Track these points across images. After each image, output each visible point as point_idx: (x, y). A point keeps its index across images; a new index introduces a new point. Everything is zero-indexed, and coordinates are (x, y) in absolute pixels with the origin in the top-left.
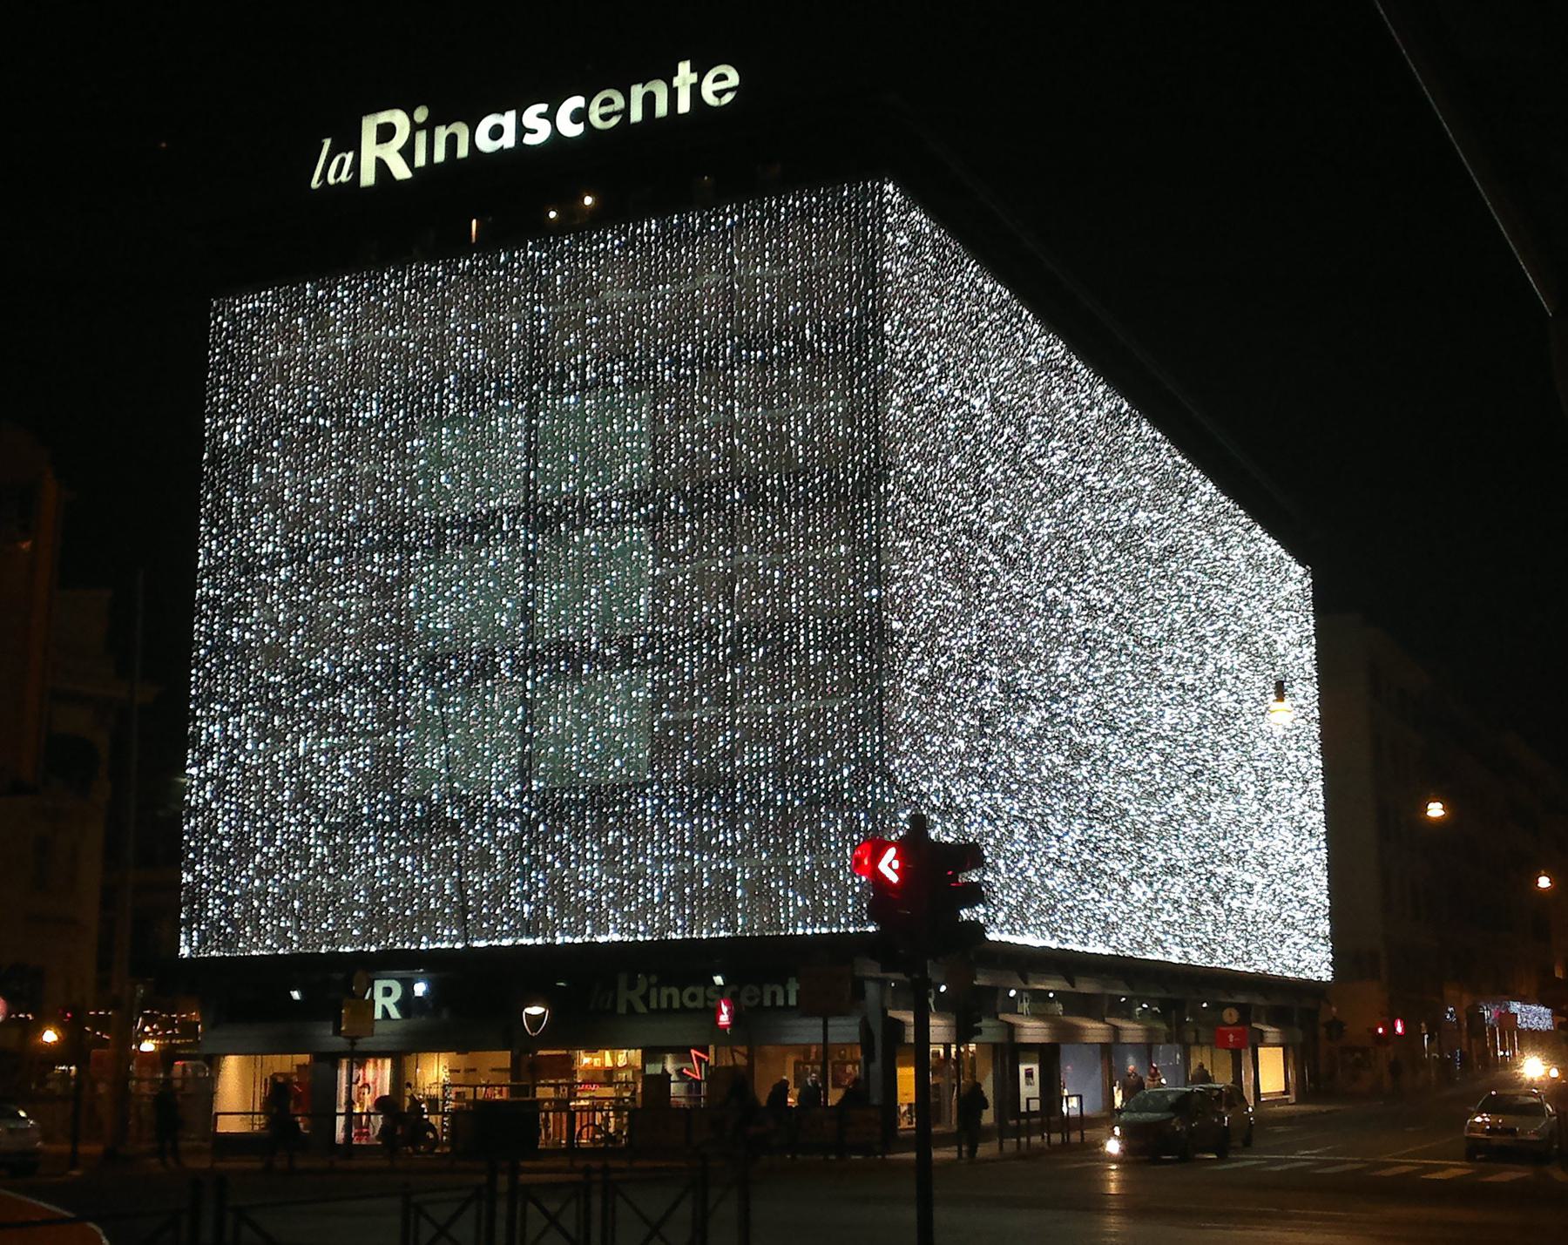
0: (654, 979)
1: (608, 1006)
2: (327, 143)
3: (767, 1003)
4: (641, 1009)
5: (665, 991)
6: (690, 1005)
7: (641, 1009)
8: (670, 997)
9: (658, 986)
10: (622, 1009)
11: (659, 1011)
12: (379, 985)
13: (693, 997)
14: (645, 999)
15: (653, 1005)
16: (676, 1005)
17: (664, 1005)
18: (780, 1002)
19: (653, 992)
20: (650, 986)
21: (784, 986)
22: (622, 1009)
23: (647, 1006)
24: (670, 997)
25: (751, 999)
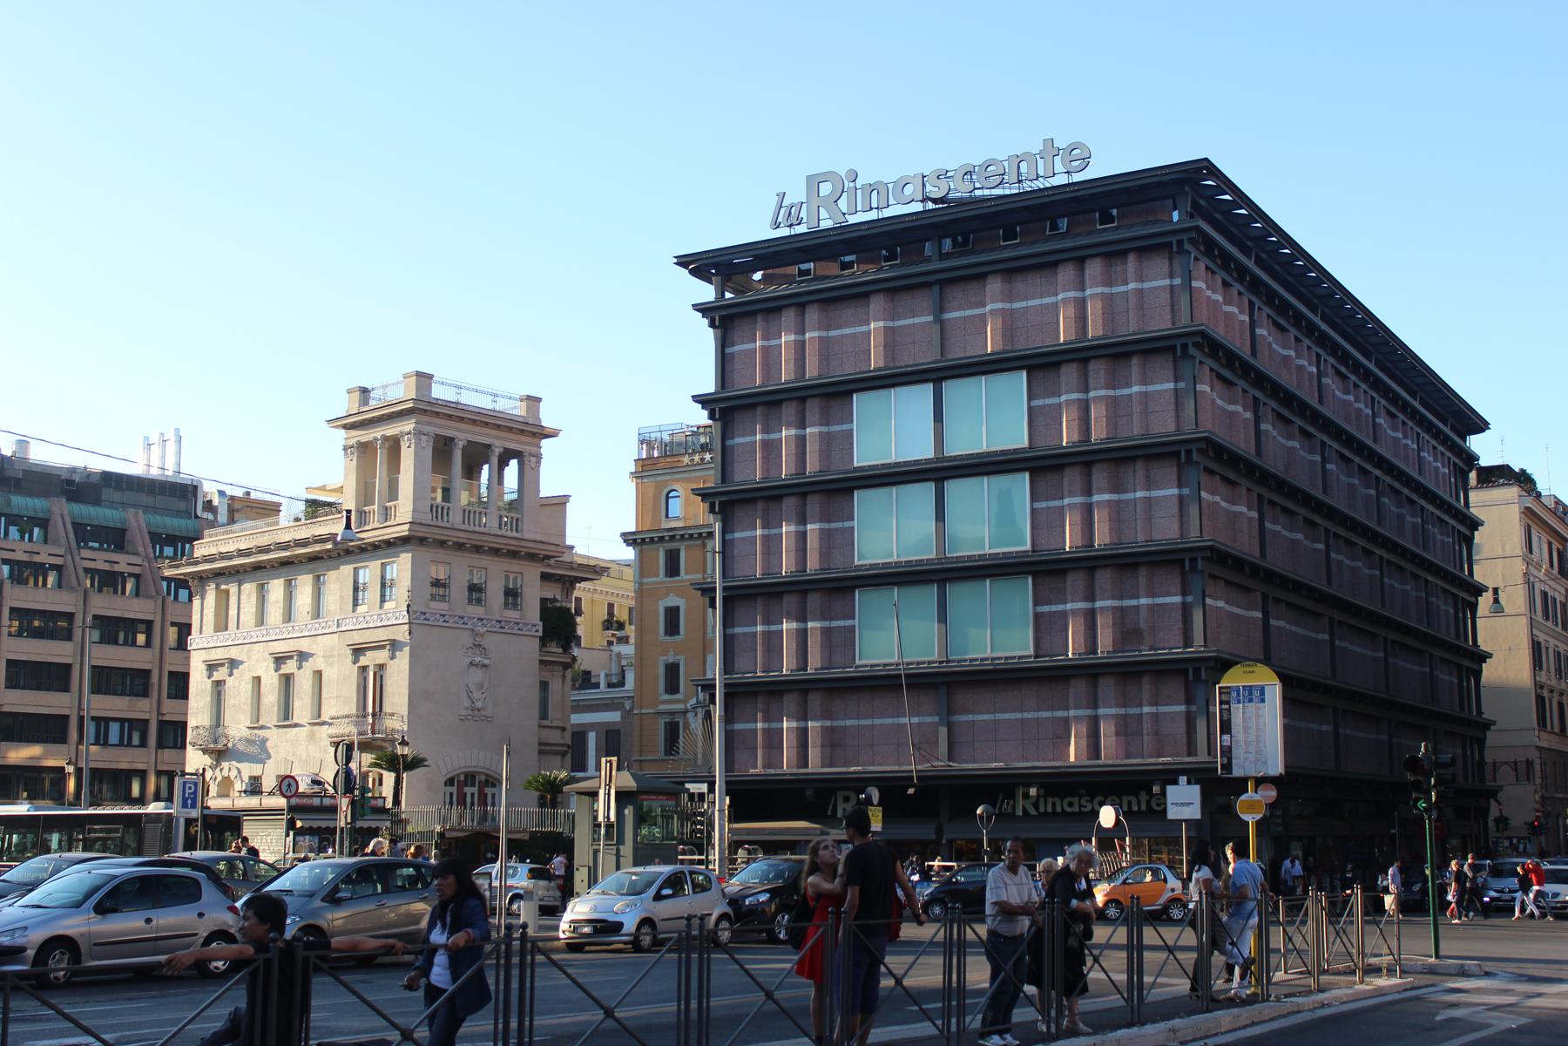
4: (1033, 812)
5: (1050, 800)
6: (1068, 809)
7: (1033, 812)
8: (1054, 805)
9: (1045, 796)
10: (1020, 813)
11: (1046, 813)
12: (840, 795)
13: (1071, 804)
14: (1036, 805)
15: (1042, 809)
16: (1059, 809)
17: (1050, 809)
19: (1042, 800)
21: (1137, 796)
24: (1054, 805)
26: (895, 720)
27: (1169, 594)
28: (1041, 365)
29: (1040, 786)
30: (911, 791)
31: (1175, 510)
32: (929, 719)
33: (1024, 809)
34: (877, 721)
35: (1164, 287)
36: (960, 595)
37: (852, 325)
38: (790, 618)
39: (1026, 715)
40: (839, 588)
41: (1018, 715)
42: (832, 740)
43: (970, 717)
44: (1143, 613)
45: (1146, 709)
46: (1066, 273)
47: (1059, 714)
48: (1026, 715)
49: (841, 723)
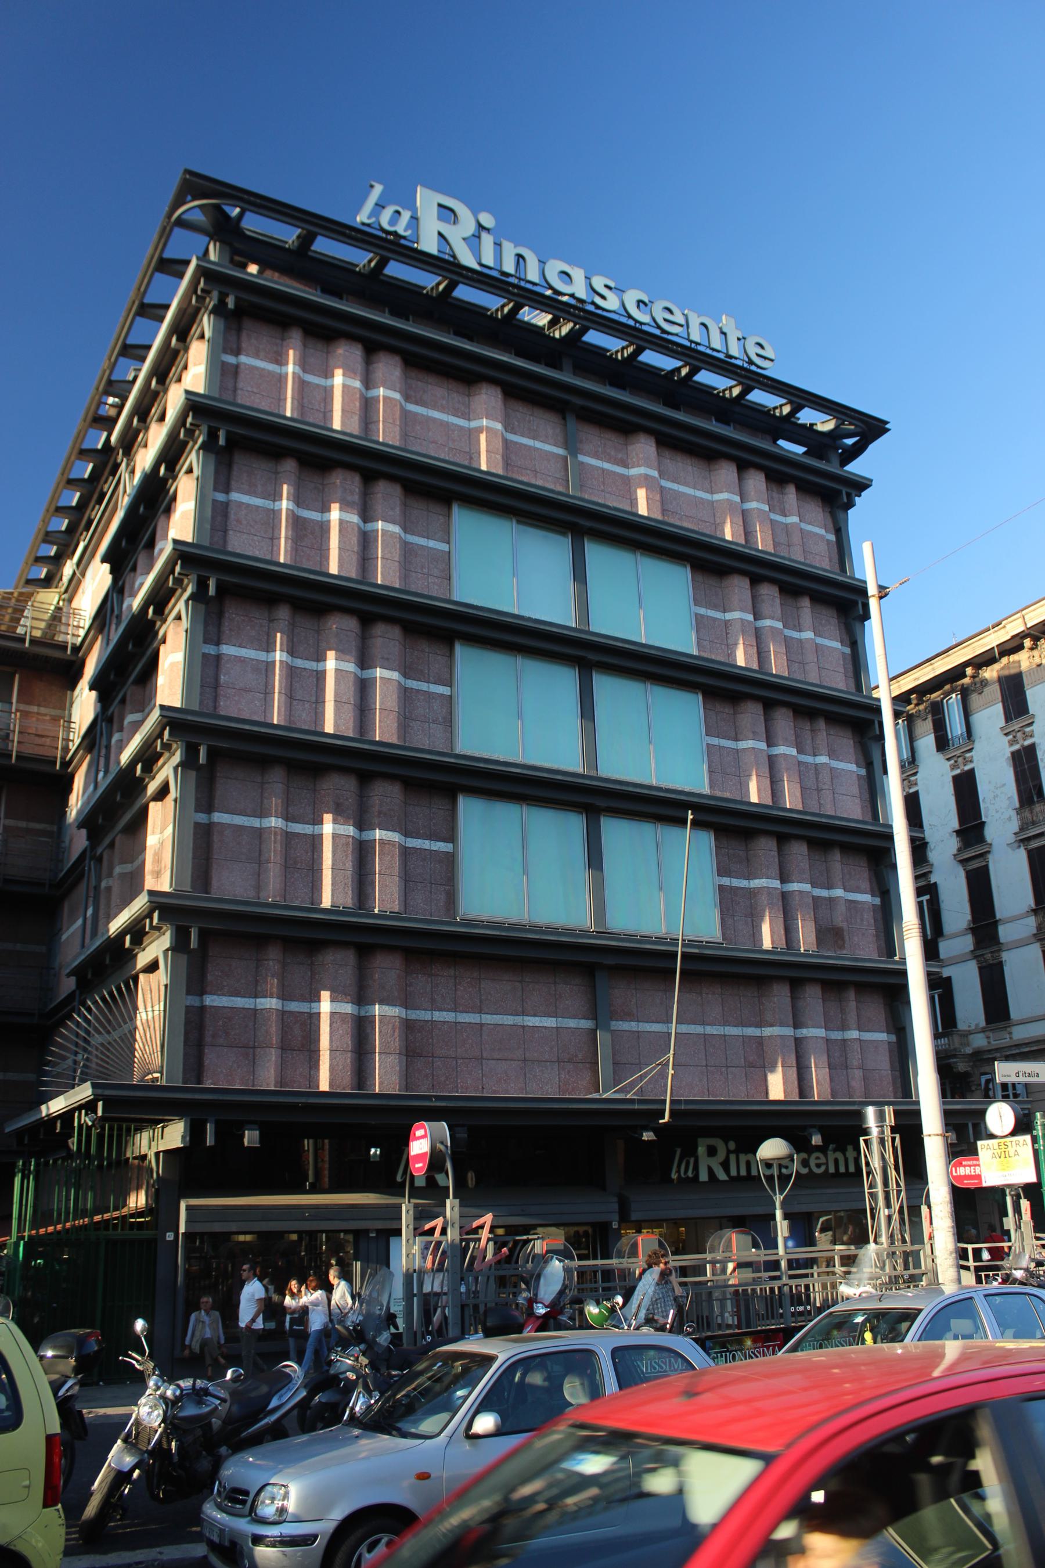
0: (732, 1145)
1: (690, 1174)
2: (378, 189)
3: (832, 1170)
4: (722, 1176)
7: (722, 1176)
9: (737, 1152)
10: (704, 1177)
11: (738, 1178)
15: (733, 1172)
17: (743, 1172)
18: (842, 1170)
19: (733, 1157)
20: (729, 1152)
21: (844, 1151)
22: (704, 1177)
23: (727, 1170)
25: (818, 1166)
26: (519, 1020)
27: (857, 890)
28: (710, 562)
29: (823, 1131)
30: (647, 1136)
31: (855, 790)
32: (572, 1023)
33: (711, 1172)
34: (488, 1019)
35: (822, 536)
36: (620, 835)
37: (442, 409)
38: (340, 814)
39: (710, 1030)
40: (436, 782)
41: (698, 1029)
42: (415, 1043)
43: (633, 1026)
44: (842, 908)
45: (854, 1034)
46: (727, 472)
47: (751, 1031)
48: (710, 1030)
49: (425, 1015)
